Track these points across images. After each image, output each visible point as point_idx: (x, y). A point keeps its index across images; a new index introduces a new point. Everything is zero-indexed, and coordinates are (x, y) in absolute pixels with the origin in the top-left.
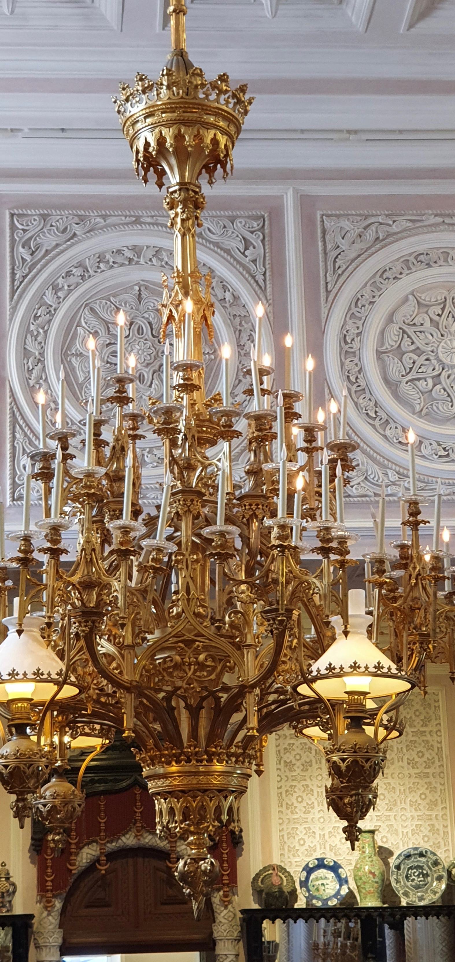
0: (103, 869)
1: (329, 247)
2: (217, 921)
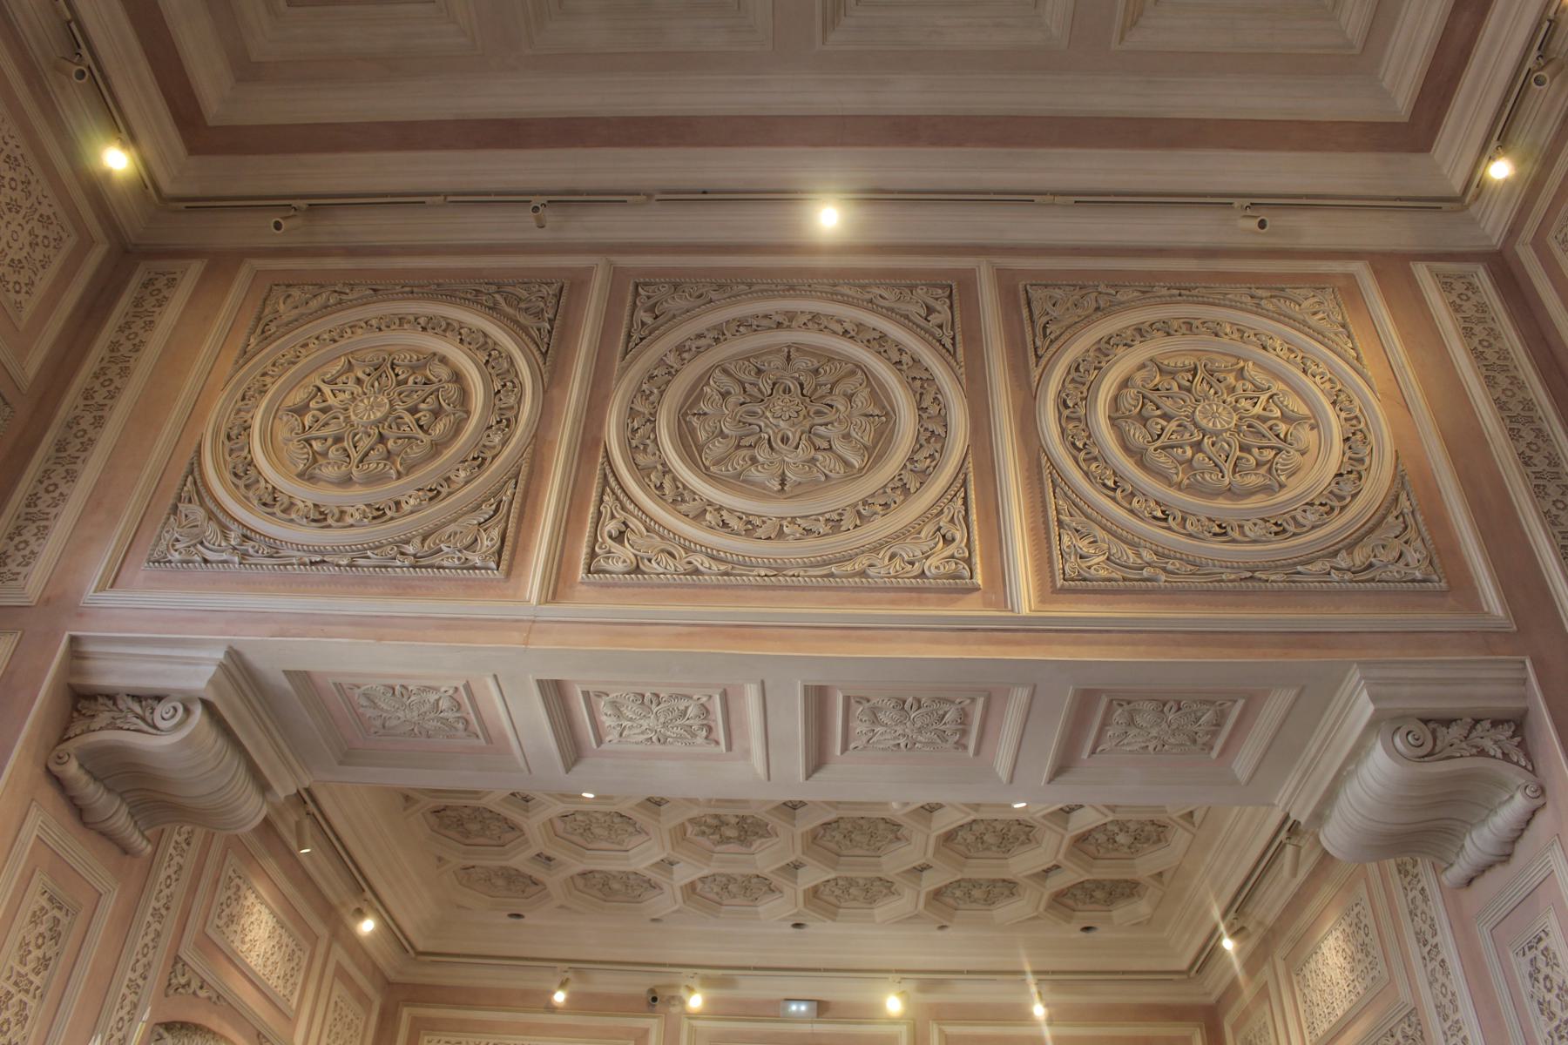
1: (1036, 313)
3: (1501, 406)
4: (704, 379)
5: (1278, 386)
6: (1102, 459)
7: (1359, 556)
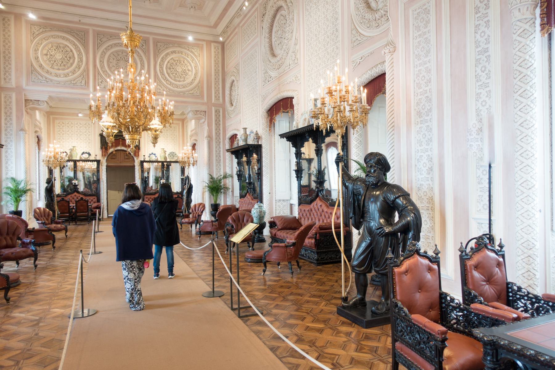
0: (114, 153)
3: (215, 70)
4: (110, 56)
5: (188, 64)
6: (164, 75)
7: (192, 92)
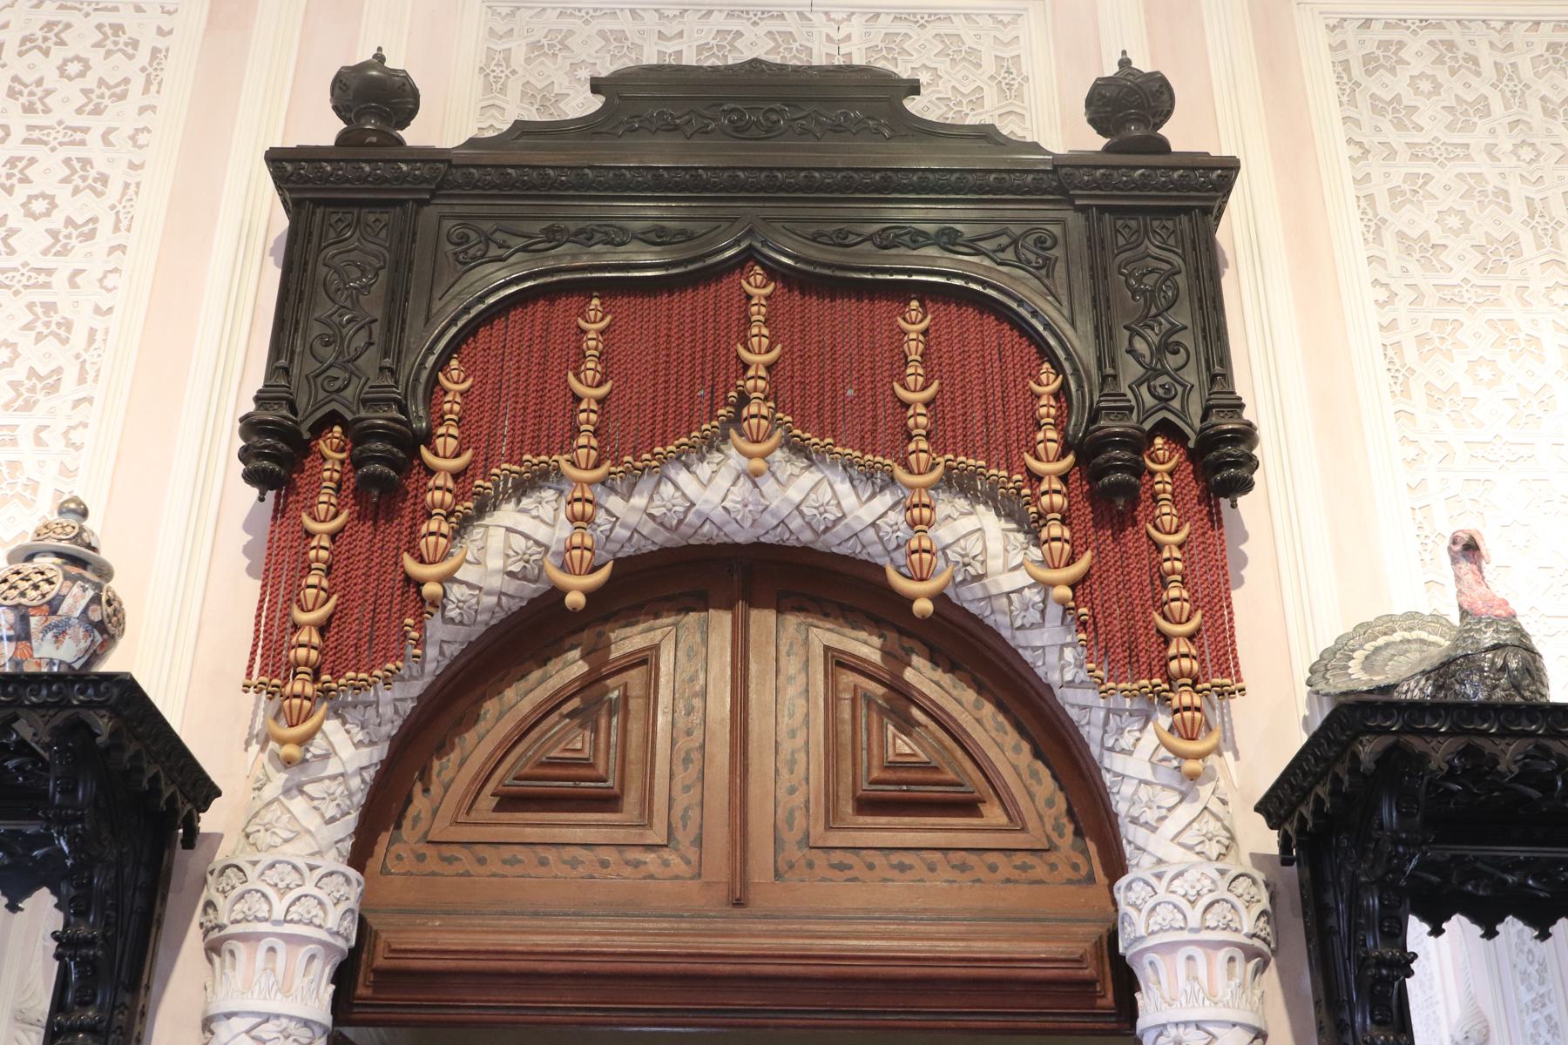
2: (1140, 866)
